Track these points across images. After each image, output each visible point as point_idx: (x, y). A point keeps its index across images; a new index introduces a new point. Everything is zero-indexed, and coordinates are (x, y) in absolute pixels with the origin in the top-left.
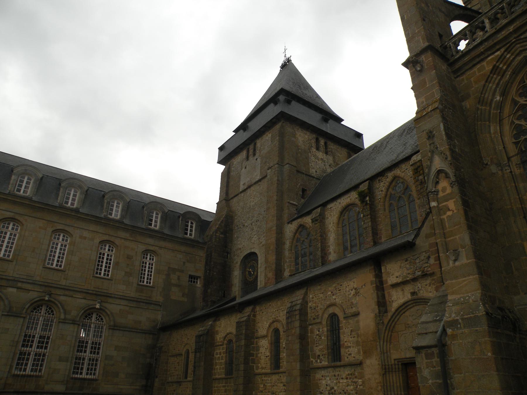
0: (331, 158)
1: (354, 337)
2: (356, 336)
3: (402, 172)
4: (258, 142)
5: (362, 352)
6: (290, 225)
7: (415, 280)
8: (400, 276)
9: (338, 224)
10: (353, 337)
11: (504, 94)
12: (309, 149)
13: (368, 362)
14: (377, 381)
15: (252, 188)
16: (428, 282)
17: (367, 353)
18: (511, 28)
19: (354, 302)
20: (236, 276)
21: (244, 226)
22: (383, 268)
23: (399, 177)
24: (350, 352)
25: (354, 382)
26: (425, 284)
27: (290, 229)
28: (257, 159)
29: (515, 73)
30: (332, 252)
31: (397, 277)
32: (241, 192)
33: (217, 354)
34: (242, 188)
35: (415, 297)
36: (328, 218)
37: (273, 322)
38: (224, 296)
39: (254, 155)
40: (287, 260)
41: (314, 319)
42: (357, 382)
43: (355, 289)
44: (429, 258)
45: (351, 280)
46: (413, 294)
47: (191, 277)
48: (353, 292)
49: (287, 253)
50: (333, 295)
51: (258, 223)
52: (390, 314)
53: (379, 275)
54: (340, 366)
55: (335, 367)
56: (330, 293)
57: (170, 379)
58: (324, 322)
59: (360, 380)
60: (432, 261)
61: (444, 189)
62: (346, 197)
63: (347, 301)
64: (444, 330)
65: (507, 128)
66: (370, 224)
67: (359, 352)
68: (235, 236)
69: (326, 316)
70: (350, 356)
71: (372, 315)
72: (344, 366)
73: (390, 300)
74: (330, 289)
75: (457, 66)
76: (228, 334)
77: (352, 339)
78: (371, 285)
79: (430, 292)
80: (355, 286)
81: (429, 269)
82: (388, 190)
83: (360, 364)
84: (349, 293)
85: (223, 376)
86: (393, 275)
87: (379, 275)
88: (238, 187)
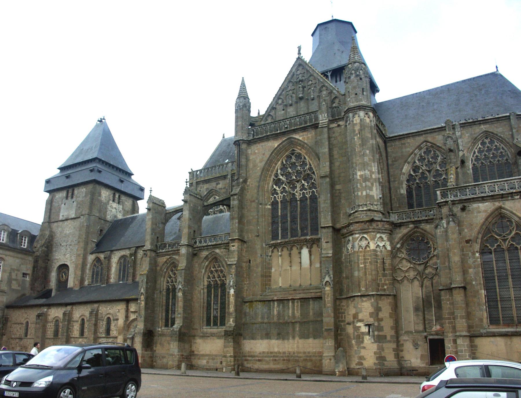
0: (121, 207)
9: (117, 263)
11: (167, 270)
12: (108, 202)
15: (68, 221)
18: (171, 252)
19: (118, 314)
20: (53, 275)
21: (61, 245)
27: (91, 258)
28: (73, 202)
29: (170, 264)
32: (60, 221)
33: (48, 326)
34: (61, 218)
37: (82, 316)
38: (45, 288)
39: (72, 197)
47: (24, 274)
48: (118, 310)
49: (88, 271)
51: (71, 247)
52: (129, 321)
53: (127, 307)
54: (109, 338)
55: (107, 338)
57: (13, 336)
58: (105, 320)
62: (124, 250)
64: (134, 335)
65: (165, 280)
66: (132, 271)
69: (106, 318)
72: (111, 338)
75: (158, 254)
76: (56, 317)
85: (53, 337)
87: (127, 307)
88: (59, 216)
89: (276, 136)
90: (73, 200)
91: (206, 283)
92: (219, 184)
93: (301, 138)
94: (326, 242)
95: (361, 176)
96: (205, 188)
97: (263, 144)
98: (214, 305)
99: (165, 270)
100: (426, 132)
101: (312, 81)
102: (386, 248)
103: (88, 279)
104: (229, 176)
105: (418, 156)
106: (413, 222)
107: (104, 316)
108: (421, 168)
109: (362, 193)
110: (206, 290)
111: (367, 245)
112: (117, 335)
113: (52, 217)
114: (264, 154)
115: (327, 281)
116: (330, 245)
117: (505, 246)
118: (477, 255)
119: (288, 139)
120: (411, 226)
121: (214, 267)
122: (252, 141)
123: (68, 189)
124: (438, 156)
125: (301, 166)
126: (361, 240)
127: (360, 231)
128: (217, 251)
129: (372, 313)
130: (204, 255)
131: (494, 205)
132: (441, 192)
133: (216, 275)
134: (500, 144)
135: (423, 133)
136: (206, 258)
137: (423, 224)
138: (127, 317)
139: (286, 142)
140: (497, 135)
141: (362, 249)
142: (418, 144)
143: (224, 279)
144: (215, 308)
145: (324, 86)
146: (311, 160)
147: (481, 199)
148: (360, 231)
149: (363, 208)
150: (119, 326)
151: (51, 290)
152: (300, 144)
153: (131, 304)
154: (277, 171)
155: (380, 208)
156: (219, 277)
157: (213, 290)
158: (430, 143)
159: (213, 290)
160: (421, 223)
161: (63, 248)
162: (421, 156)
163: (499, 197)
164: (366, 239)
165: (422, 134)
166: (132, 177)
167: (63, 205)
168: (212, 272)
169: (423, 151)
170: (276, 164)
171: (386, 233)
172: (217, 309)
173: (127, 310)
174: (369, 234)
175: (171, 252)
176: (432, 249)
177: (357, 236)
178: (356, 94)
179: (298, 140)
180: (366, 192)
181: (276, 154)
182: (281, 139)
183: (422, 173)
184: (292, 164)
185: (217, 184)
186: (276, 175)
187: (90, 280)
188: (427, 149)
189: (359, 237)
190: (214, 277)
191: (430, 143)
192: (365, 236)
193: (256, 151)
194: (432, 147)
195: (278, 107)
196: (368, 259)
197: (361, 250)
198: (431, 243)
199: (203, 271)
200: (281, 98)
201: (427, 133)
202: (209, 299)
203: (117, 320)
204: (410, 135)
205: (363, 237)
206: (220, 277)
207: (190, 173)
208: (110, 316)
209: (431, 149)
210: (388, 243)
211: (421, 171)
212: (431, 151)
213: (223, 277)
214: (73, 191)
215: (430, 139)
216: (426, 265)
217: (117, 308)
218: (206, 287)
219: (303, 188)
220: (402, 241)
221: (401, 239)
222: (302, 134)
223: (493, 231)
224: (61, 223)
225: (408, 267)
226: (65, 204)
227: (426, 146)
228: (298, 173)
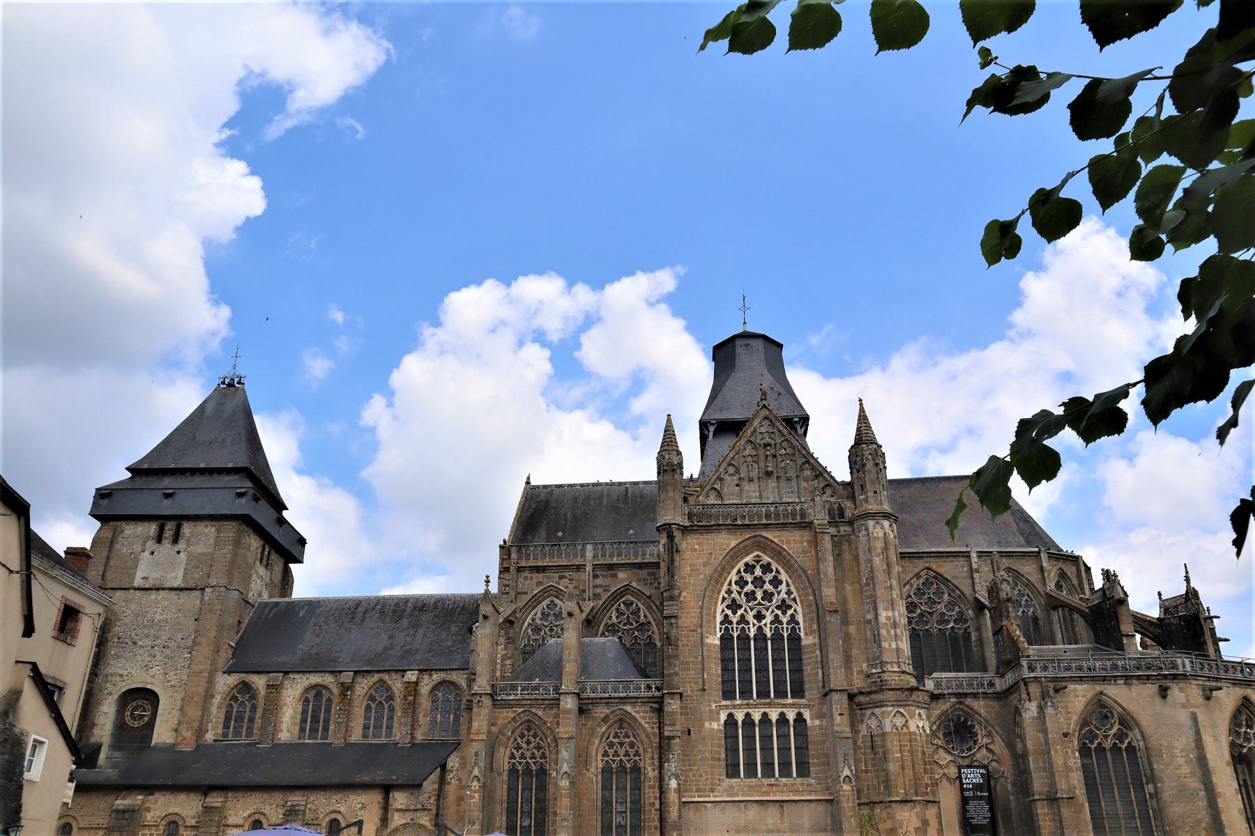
0: (269, 574)
3: (391, 680)
4: (186, 525)
6: (226, 675)
7: (416, 810)
9: (299, 700)
11: (512, 733)
12: (254, 563)
15: (161, 592)
16: (426, 814)
18: (529, 702)
21: (135, 643)
23: (385, 682)
27: (225, 682)
28: (179, 552)
29: (521, 724)
30: (285, 730)
32: (135, 589)
34: (138, 582)
36: (287, 689)
37: (255, 813)
39: (176, 540)
40: (214, 720)
41: (313, 820)
44: (430, 798)
45: (359, 796)
46: (412, 819)
48: (360, 806)
49: (214, 710)
50: (338, 803)
51: (168, 652)
52: (389, 831)
53: (386, 799)
56: (334, 801)
58: (324, 825)
60: (432, 800)
61: (475, 786)
62: (318, 675)
65: (508, 752)
68: (113, 653)
69: (327, 819)
71: (375, 828)
74: (335, 797)
75: (496, 703)
76: (170, 814)
82: (370, 689)
87: (386, 799)
88: (132, 576)
89: (734, 528)
90: (177, 548)
91: (600, 765)
93: (776, 540)
94: (840, 714)
95: (888, 618)
97: (709, 536)
98: (618, 805)
99: (509, 734)
100: (929, 555)
101: (785, 449)
102: (925, 731)
103: (215, 728)
104: (589, 568)
105: (915, 586)
106: (956, 695)
107: (321, 816)
108: (920, 607)
109: (890, 645)
110: (600, 778)
111: (904, 725)
113: (109, 576)
114: (711, 554)
115: (847, 776)
116: (846, 718)
117: (1108, 744)
118: (1077, 754)
119: (755, 536)
120: (953, 700)
121: (616, 736)
122: (689, 529)
123: (162, 521)
124: (943, 593)
125: (771, 582)
126: (895, 716)
127: (894, 703)
128: (628, 708)
129: (919, 828)
130: (601, 713)
131: (1094, 689)
132: (1027, 664)
133: (622, 752)
134: (1025, 587)
135: (925, 555)
136: (605, 719)
137: (969, 700)
138: (384, 821)
139: (749, 541)
140: (1023, 576)
141: (897, 730)
142: (917, 570)
143: (637, 758)
144: (618, 810)
145: (808, 462)
146: (791, 578)
147: (1079, 679)
148: (894, 703)
149: (892, 667)
151: (98, 748)
154: (730, 584)
155: (910, 669)
156: (627, 754)
157: (614, 777)
158: (934, 571)
159: (614, 777)
160: (966, 697)
161: (141, 651)
162: (919, 589)
163: (1101, 678)
164: (903, 715)
165: (923, 557)
166: (285, 513)
167: (147, 554)
168: (611, 745)
169: (921, 581)
170: (729, 573)
171: (924, 708)
172: (625, 812)
173: (386, 807)
174: (907, 708)
175: (529, 702)
176: (979, 736)
177: (890, 709)
178: (875, 492)
179: (773, 542)
180: (897, 645)
181: (731, 558)
182: (741, 535)
183: (921, 613)
184: (755, 578)
186: (729, 592)
187: (220, 731)
188: (927, 579)
189: (891, 712)
190: (616, 754)
191: (934, 571)
192: (900, 710)
193: (697, 547)
194: (934, 577)
195: (726, 477)
196: (907, 746)
197: (894, 731)
198: (977, 727)
199: (597, 741)
200: (733, 465)
201: (931, 557)
202: (607, 794)
204: (906, 555)
205: (898, 712)
206: (629, 756)
207: (501, 547)
208: (339, 817)
209: (933, 580)
210: (927, 723)
211: (918, 611)
212: (932, 583)
213: (635, 756)
214: (179, 527)
215: (934, 567)
216: (972, 758)
218: (600, 770)
219: (776, 620)
220: (939, 721)
221: (939, 718)
222: (777, 533)
223: (1092, 723)
224: (138, 593)
225: (948, 760)
226: (152, 553)
227: (927, 574)
228: (768, 596)
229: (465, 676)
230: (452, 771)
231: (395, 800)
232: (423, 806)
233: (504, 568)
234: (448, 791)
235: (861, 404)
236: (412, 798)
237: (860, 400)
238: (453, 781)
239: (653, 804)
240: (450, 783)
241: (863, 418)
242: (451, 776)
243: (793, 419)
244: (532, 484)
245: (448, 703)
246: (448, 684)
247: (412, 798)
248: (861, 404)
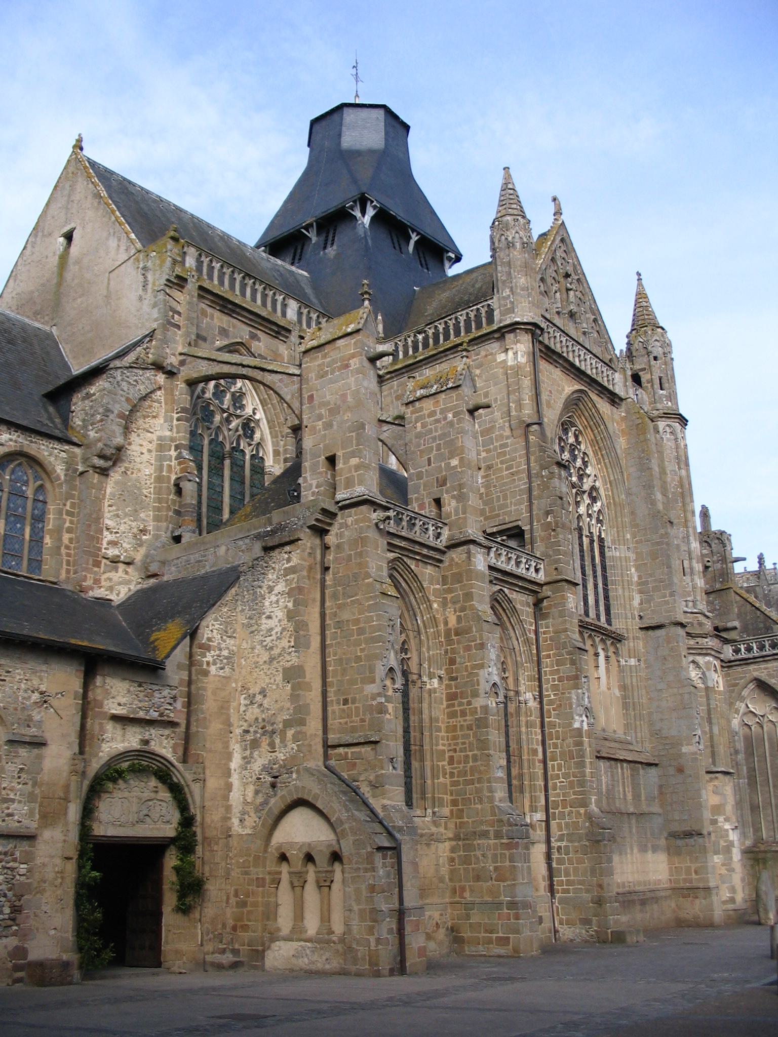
1: (25, 784)
2: (30, 783)
5: (37, 816)
7: (150, 723)
8: (125, 705)
10: (24, 784)
13: (47, 834)
14: (56, 869)
17: (48, 818)
18: (403, 544)
22: (99, 680)
24: (10, 811)
25: (8, 868)
26: (160, 732)
31: (119, 704)
35: (146, 748)
42: (16, 868)
43: (42, 693)
44: (174, 698)
48: (36, 697)
59: (22, 866)
60: (179, 705)
63: (19, 709)
67: (31, 813)
70: (11, 818)
73: (100, 737)
77: (20, 786)
78: (75, 699)
79: (165, 748)
80: (43, 688)
81: (172, 715)
83: (31, 838)
84: (26, 695)
86: (113, 698)
92: (259, 340)
96: (217, 323)
112: (32, 825)
150: (44, 777)
152: (592, 417)
153: (109, 680)
173: (86, 707)
175: (403, 544)
185: (253, 337)
203: (39, 744)
217: (36, 682)
229: (63, 455)
230: (208, 648)
231: (107, 693)
232: (161, 715)
233: (178, 277)
234: (205, 689)
235: (639, 280)
236: (141, 695)
237: (639, 274)
238: (213, 669)
239: (535, 752)
240: (206, 673)
241: (641, 297)
242: (209, 657)
243: (448, 252)
244: (85, 152)
245: (20, 501)
246: (22, 460)
247: (141, 695)
248: (639, 280)
